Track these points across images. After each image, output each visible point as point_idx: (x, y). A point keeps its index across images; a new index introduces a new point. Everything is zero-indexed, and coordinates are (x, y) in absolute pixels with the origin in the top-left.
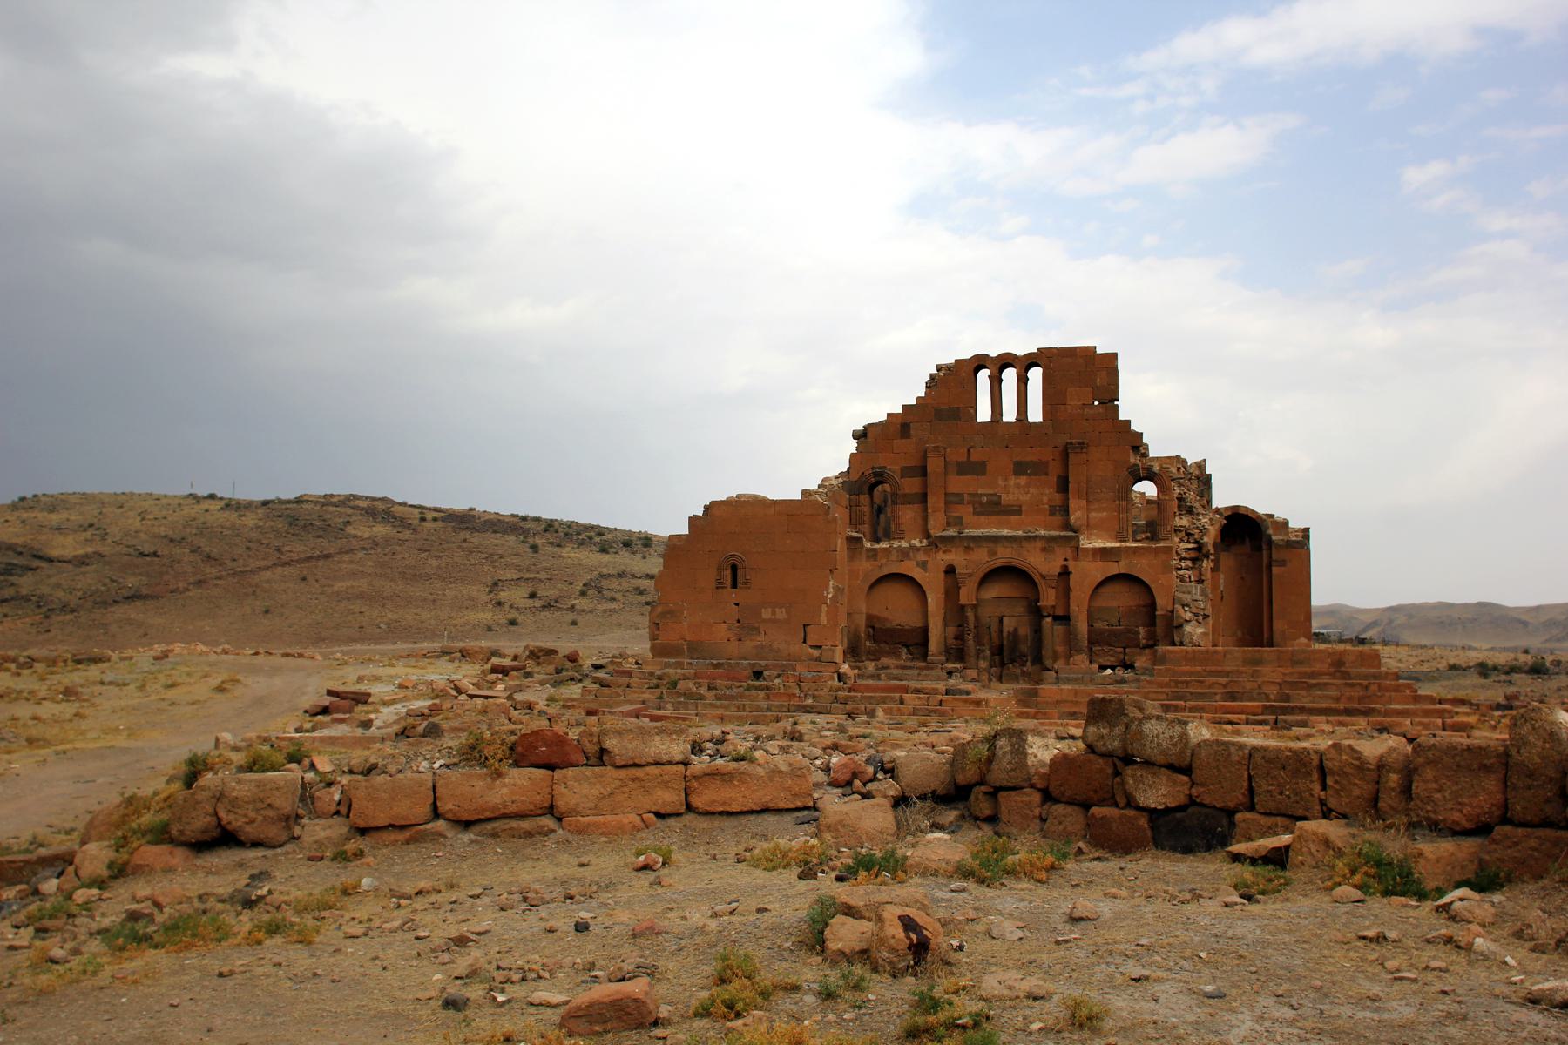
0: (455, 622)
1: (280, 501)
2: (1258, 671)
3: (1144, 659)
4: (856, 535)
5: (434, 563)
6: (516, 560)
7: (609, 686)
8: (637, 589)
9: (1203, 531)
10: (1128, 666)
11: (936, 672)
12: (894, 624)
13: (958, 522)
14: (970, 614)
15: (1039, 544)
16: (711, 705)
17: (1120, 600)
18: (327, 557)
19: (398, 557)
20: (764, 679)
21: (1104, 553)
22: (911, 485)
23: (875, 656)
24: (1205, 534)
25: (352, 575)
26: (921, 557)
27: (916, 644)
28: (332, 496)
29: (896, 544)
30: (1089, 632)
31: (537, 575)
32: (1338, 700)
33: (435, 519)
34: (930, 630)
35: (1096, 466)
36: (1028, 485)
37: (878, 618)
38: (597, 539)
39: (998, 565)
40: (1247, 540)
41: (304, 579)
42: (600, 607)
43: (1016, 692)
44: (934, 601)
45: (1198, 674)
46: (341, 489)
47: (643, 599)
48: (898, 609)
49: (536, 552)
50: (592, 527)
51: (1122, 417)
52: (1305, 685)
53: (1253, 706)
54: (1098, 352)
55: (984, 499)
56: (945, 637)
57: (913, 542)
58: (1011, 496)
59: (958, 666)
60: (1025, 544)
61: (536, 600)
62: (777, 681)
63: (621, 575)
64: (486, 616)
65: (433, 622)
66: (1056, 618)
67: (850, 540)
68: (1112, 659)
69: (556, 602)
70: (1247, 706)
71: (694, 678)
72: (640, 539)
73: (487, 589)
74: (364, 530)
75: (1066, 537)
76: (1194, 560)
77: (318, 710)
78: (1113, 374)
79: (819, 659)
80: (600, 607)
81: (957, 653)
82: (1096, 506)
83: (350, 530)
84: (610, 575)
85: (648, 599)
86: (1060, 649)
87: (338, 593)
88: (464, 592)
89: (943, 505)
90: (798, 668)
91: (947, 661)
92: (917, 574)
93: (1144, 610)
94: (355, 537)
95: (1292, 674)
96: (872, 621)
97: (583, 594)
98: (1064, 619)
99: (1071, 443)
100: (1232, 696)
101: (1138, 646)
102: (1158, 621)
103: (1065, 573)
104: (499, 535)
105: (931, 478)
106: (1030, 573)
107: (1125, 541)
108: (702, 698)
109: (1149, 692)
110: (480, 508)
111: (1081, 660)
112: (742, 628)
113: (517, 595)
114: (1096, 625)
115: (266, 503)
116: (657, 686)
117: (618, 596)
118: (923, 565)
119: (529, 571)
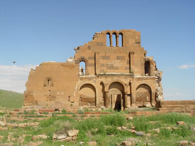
3: (148, 105)
10: (144, 106)
15: (124, 77)
21: (139, 79)
29: (87, 76)
34: (97, 97)
36: (120, 62)
37: (83, 95)
39: (114, 82)
48: (88, 93)
55: (109, 65)
57: (92, 76)
60: (121, 76)
68: (141, 105)
76: (157, 81)
78: (139, 36)
92: (93, 84)
98: (130, 95)
99: (131, 52)
102: (152, 95)
114: (137, 96)
118: (95, 82)
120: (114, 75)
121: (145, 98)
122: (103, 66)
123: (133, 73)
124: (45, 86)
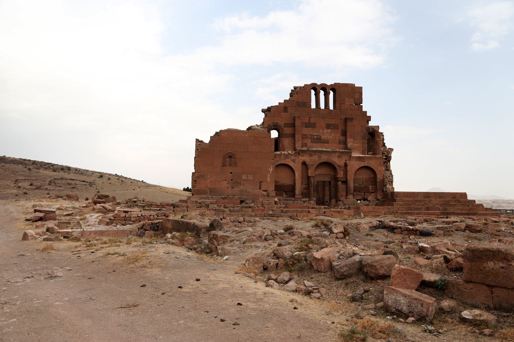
0: (3, 193)
2: (431, 200)
6: (23, 173)
7: (178, 207)
8: (68, 183)
10: (365, 200)
12: (281, 183)
13: (305, 145)
14: (312, 180)
15: (337, 154)
16: (230, 214)
17: (365, 175)
20: (247, 204)
21: (359, 158)
22: (288, 131)
24: (389, 153)
27: (289, 191)
29: (283, 153)
31: (32, 178)
32: (462, 210)
34: (296, 184)
35: (354, 128)
38: (52, 167)
42: (56, 189)
44: (298, 175)
47: (71, 186)
49: (30, 171)
50: (50, 164)
51: (363, 110)
52: (449, 205)
53: (437, 212)
54: (356, 86)
55: (315, 137)
57: (289, 152)
58: (325, 136)
59: (307, 199)
60: (332, 154)
61: (33, 186)
62: (252, 205)
63: (62, 179)
64: (15, 191)
66: (342, 182)
68: (360, 197)
69: (40, 187)
70: (435, 212)
71: (216, 204)
72: (66, 168)
73: (14, 182)
75: (347, 152)
77: (37, 219)
80: (56, 189)
82: (355, 141)
84: (58, 179)
85: (73, 187)
88: (5, 183)
89: (301, 138)
90: (260, 199)
92: (291, 164)
95: (442, 201)
97: (50, 184)
98: (345, 182)
99: (348, 118)
100: (428, 209)
101: (369, 193)
102: (378, 184)
104: (16, 165)
105: (297, 128)
107: (365, 154)
108: (224, 211)
109: (400, 207)
110: (7, 156)
111: (351, 197)
113: (26, 184)
114: (355, 185)
116: (201, 207)
117: (62, 185)
118: (294, 161)
119: (28, 177)
120: (321, 152)
122: (306, 138)
123: (350, 150)
124: (224, 165)
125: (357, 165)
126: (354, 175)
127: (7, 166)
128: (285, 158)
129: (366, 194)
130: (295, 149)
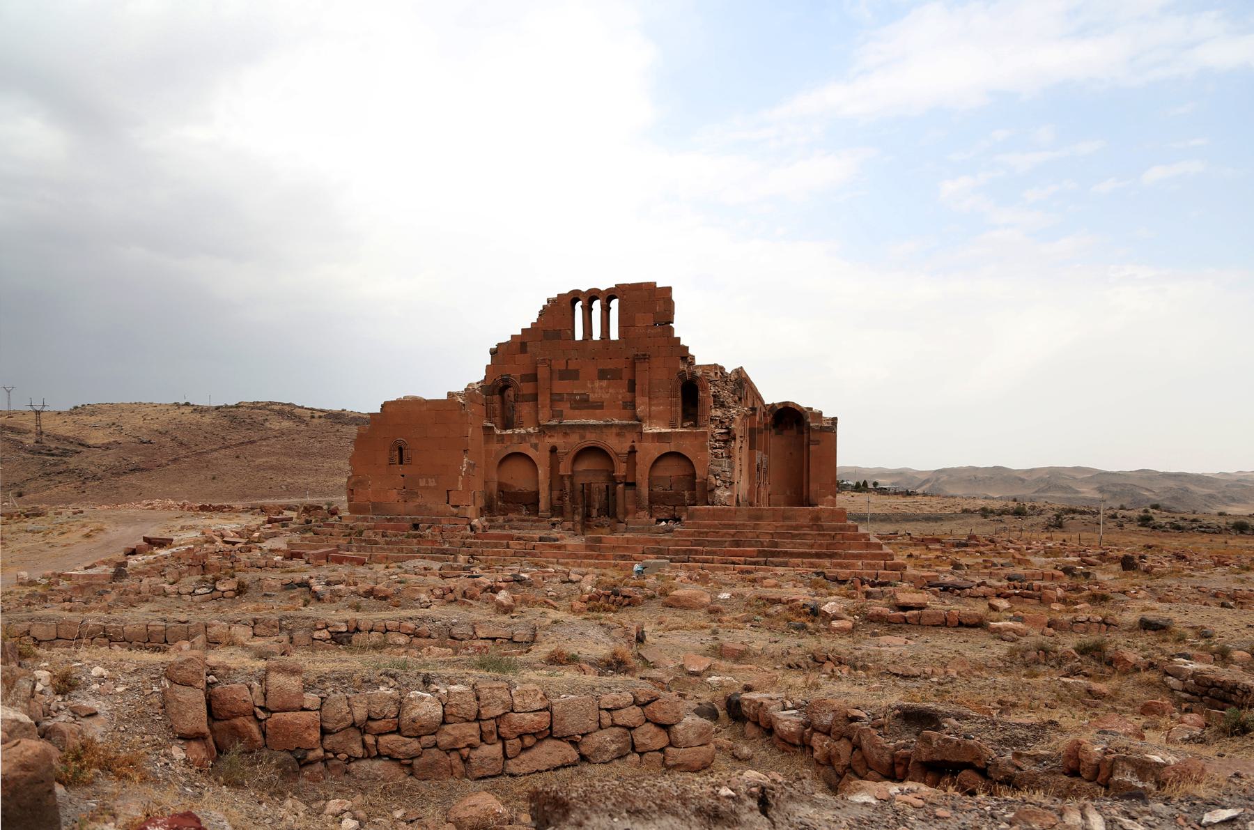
1: (227, 407)
4: (489, 425)
5: (318, 445)
9: (732, 420)
11: (545, 524)
14: (567, 483)
15: (614, 430)
17: (670, 471)
18: (253, 442)
19: (296, 442)
21: (660, 437)
22: (527, 388)
23: (504, 512)
25: (267, 454)
26: (534, 440)
28: (258, 402)
29: (517, 431)
30: (650, 494)
33: (320, 417)
37: (506, 485)
40: (795, 425)
41: (238, 457)
43: (586, 539)
44: (543, 472)
45: (715, 526)
46: (264, 398)
48: (518, 479)
55: (578, 398)
56: (551, 499)
57: (529, 429)
58: (596, 395)
59: (559, 519)
60: (604, 431)
65: (314, 484)
66: (627, 484)
67: (486, 428)
74: (276, 424)
75: (632, 425)
76: (725, 442)
79: (456, 515)
81: (557, 510)
82: (655, 402)
83: (267, 424)
86: (629, 507)
87: (258, 466)
89: (548, 401)
91: (552, 516)
92: (531, 453)
93: (689, 478)
94: (270, 429)
96: (501, 486)
98: (633, 485)
103: (633, 452)
106: (608, 452)
110: (349, 410)
112: (406, 492)
115: (217, 408)
118: (535, 446)
121: (678, 494)
122: (562, 400)
125: (656, 450)
126: (648, 470)
127: (344, 430)
128: (520, 441)
129: (677, 508)
130: (539, 425)
